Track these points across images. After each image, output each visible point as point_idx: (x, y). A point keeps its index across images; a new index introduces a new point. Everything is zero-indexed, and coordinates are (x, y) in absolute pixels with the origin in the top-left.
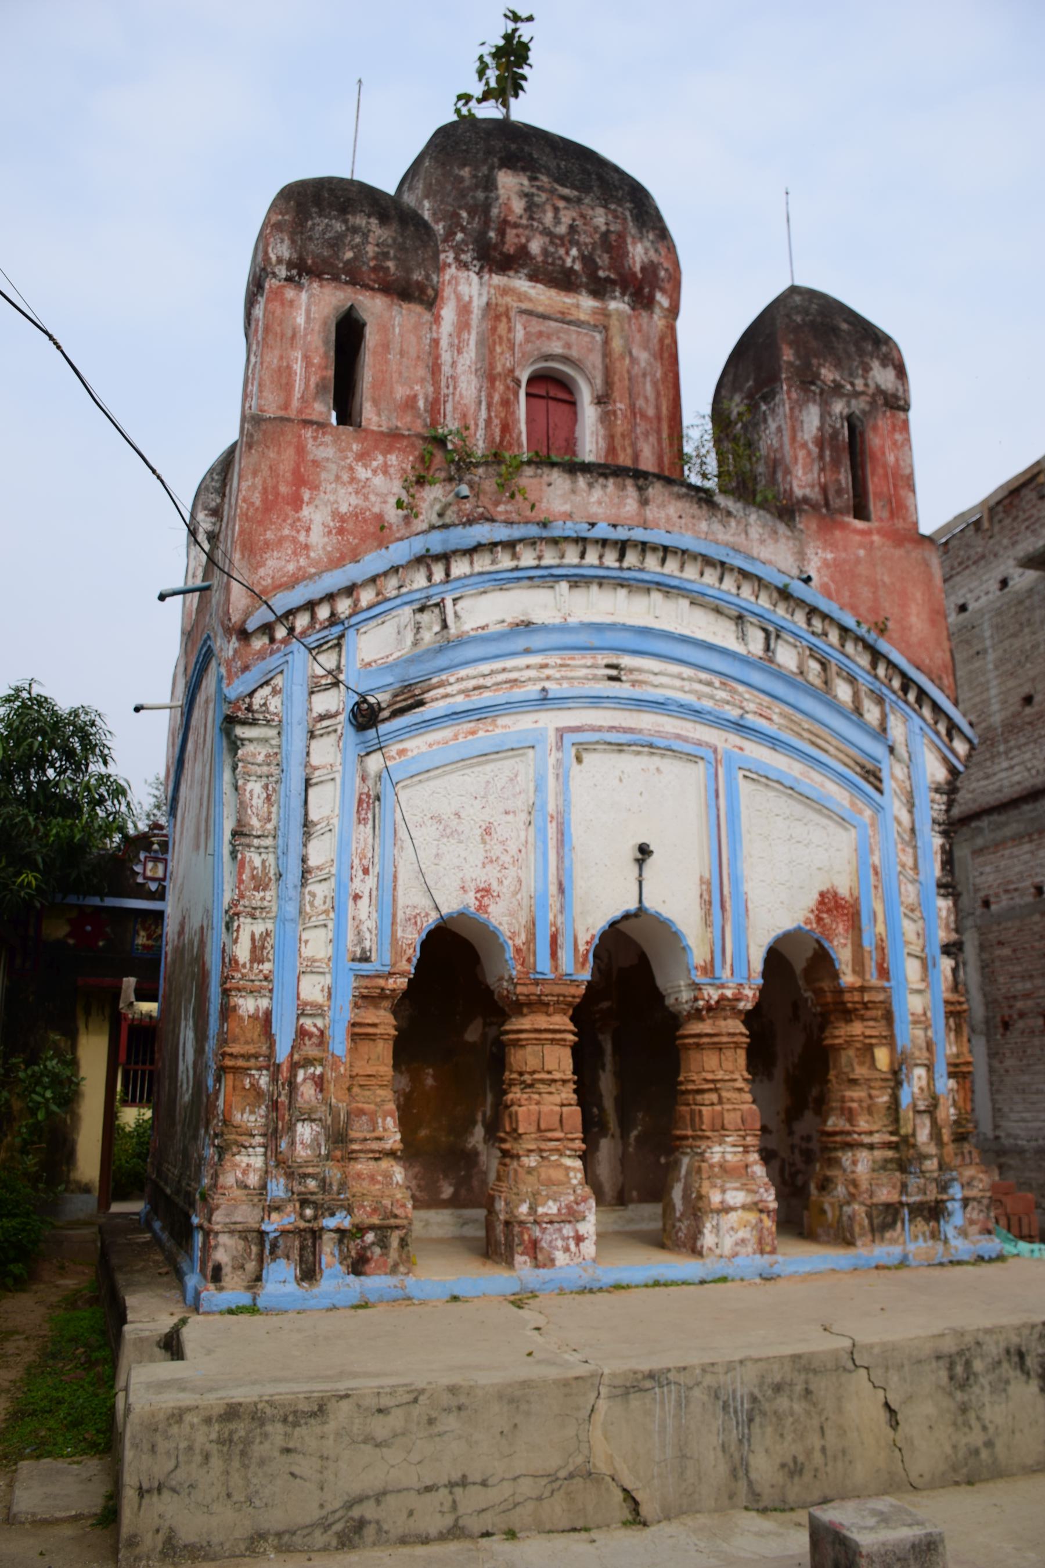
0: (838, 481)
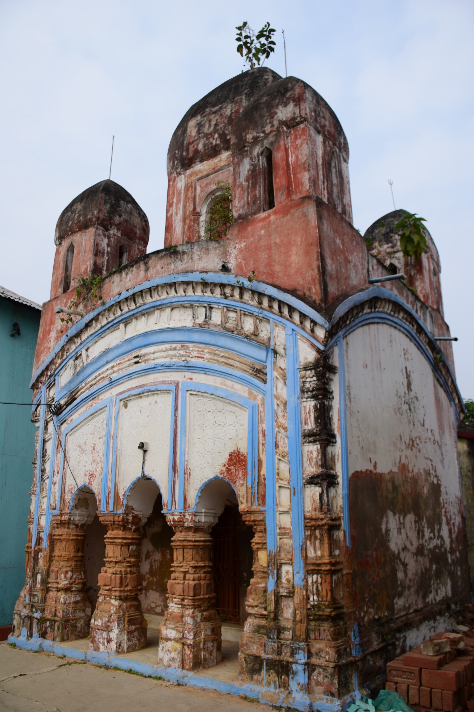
0: (255, 195)
